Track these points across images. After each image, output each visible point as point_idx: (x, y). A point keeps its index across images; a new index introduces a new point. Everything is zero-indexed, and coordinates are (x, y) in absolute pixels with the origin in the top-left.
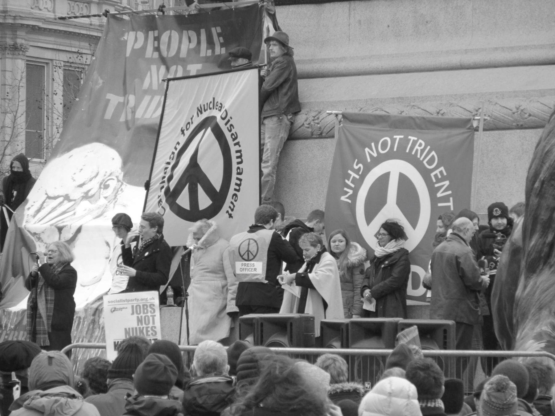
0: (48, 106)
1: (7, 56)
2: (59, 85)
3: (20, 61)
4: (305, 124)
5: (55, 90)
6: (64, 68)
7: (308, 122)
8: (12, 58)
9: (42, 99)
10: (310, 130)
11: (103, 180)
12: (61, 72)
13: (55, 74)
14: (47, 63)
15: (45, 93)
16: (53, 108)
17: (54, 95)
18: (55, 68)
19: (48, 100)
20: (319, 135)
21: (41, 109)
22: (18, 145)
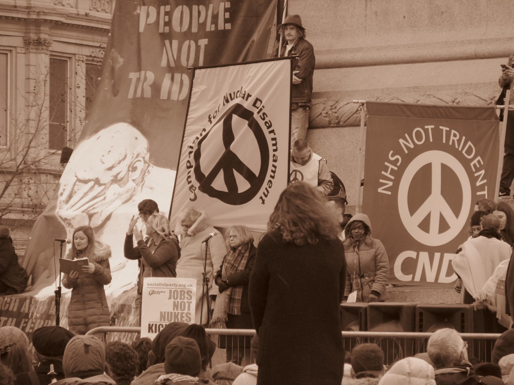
0: (71, 99)
1: (31, 51)
2: (82, 78)
3: (43, 55)
4: (322, 113)
5: (78, 83)
6: (87, 62)
7: (325, 111)
8: (36, 53)
9: (65, 93)
10: (327, 119)
11: (132, 163)
12: (84, 65)
13: (78, 67)
14: (70, 58)
15: (67, 86)
16: (75, 101)
17: (77, 88)
18: (78, 62)
19: (71, 93)
20: (336, 124)
21: (64, 102)
22: (43, 139)
